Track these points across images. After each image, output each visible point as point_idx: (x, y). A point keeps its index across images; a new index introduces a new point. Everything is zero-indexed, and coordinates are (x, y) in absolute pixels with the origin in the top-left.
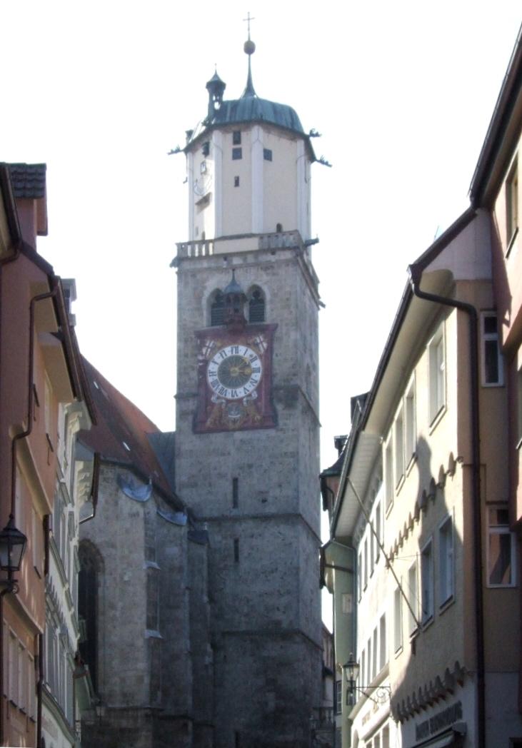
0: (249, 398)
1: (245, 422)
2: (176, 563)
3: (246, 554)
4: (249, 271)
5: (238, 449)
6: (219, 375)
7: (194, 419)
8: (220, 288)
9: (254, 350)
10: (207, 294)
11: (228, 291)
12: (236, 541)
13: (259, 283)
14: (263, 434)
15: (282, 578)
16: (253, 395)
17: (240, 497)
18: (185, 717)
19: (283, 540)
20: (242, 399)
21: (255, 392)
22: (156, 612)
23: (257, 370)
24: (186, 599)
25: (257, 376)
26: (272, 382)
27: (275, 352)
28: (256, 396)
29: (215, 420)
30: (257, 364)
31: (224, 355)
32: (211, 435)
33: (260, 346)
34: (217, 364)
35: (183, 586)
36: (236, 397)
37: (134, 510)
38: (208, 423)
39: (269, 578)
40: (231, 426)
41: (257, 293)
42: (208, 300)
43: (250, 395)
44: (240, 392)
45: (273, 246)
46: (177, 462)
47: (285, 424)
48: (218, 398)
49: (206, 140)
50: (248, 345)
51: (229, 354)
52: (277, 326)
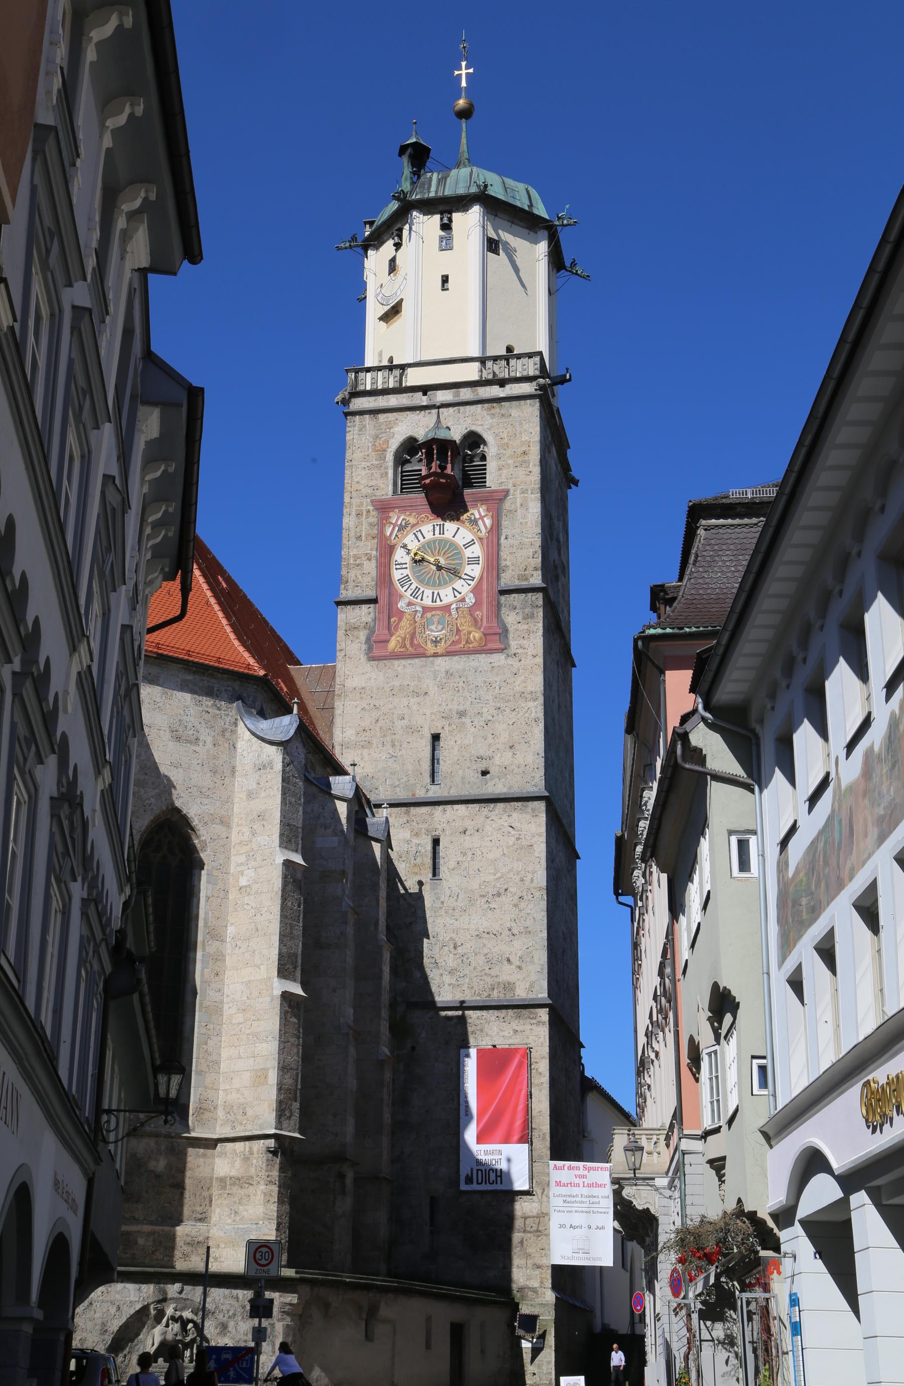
3: (452, 864)
7: (368, 640)
8: (416, 436)
9: (470, 531)
10: (394, 444)
11: (430, 436)
12: (436, 842)
14: (483, 660)
15: (516, 906)
17: (443, 767)
18: (339, 1158)
19: (518, 839)
21: (472, 595)
23: (474, 561)
25: (476, 571)
26: (498, 578)
27: (504, 532)
28: (473, 601)
29: (404, 639)
30: (476, 551)
31: (420, 537)
32: (396, 662)
33: (480, 523)
36: (438, 603)
37: (264, 758)
38: (392, 644)
39: (492, 906)
40: (431, 649)
41: (474, 440)
44: (447, 596)
45: (501, 376)
49: (399, 226)
51: (429, 536)
52: (506, 493)
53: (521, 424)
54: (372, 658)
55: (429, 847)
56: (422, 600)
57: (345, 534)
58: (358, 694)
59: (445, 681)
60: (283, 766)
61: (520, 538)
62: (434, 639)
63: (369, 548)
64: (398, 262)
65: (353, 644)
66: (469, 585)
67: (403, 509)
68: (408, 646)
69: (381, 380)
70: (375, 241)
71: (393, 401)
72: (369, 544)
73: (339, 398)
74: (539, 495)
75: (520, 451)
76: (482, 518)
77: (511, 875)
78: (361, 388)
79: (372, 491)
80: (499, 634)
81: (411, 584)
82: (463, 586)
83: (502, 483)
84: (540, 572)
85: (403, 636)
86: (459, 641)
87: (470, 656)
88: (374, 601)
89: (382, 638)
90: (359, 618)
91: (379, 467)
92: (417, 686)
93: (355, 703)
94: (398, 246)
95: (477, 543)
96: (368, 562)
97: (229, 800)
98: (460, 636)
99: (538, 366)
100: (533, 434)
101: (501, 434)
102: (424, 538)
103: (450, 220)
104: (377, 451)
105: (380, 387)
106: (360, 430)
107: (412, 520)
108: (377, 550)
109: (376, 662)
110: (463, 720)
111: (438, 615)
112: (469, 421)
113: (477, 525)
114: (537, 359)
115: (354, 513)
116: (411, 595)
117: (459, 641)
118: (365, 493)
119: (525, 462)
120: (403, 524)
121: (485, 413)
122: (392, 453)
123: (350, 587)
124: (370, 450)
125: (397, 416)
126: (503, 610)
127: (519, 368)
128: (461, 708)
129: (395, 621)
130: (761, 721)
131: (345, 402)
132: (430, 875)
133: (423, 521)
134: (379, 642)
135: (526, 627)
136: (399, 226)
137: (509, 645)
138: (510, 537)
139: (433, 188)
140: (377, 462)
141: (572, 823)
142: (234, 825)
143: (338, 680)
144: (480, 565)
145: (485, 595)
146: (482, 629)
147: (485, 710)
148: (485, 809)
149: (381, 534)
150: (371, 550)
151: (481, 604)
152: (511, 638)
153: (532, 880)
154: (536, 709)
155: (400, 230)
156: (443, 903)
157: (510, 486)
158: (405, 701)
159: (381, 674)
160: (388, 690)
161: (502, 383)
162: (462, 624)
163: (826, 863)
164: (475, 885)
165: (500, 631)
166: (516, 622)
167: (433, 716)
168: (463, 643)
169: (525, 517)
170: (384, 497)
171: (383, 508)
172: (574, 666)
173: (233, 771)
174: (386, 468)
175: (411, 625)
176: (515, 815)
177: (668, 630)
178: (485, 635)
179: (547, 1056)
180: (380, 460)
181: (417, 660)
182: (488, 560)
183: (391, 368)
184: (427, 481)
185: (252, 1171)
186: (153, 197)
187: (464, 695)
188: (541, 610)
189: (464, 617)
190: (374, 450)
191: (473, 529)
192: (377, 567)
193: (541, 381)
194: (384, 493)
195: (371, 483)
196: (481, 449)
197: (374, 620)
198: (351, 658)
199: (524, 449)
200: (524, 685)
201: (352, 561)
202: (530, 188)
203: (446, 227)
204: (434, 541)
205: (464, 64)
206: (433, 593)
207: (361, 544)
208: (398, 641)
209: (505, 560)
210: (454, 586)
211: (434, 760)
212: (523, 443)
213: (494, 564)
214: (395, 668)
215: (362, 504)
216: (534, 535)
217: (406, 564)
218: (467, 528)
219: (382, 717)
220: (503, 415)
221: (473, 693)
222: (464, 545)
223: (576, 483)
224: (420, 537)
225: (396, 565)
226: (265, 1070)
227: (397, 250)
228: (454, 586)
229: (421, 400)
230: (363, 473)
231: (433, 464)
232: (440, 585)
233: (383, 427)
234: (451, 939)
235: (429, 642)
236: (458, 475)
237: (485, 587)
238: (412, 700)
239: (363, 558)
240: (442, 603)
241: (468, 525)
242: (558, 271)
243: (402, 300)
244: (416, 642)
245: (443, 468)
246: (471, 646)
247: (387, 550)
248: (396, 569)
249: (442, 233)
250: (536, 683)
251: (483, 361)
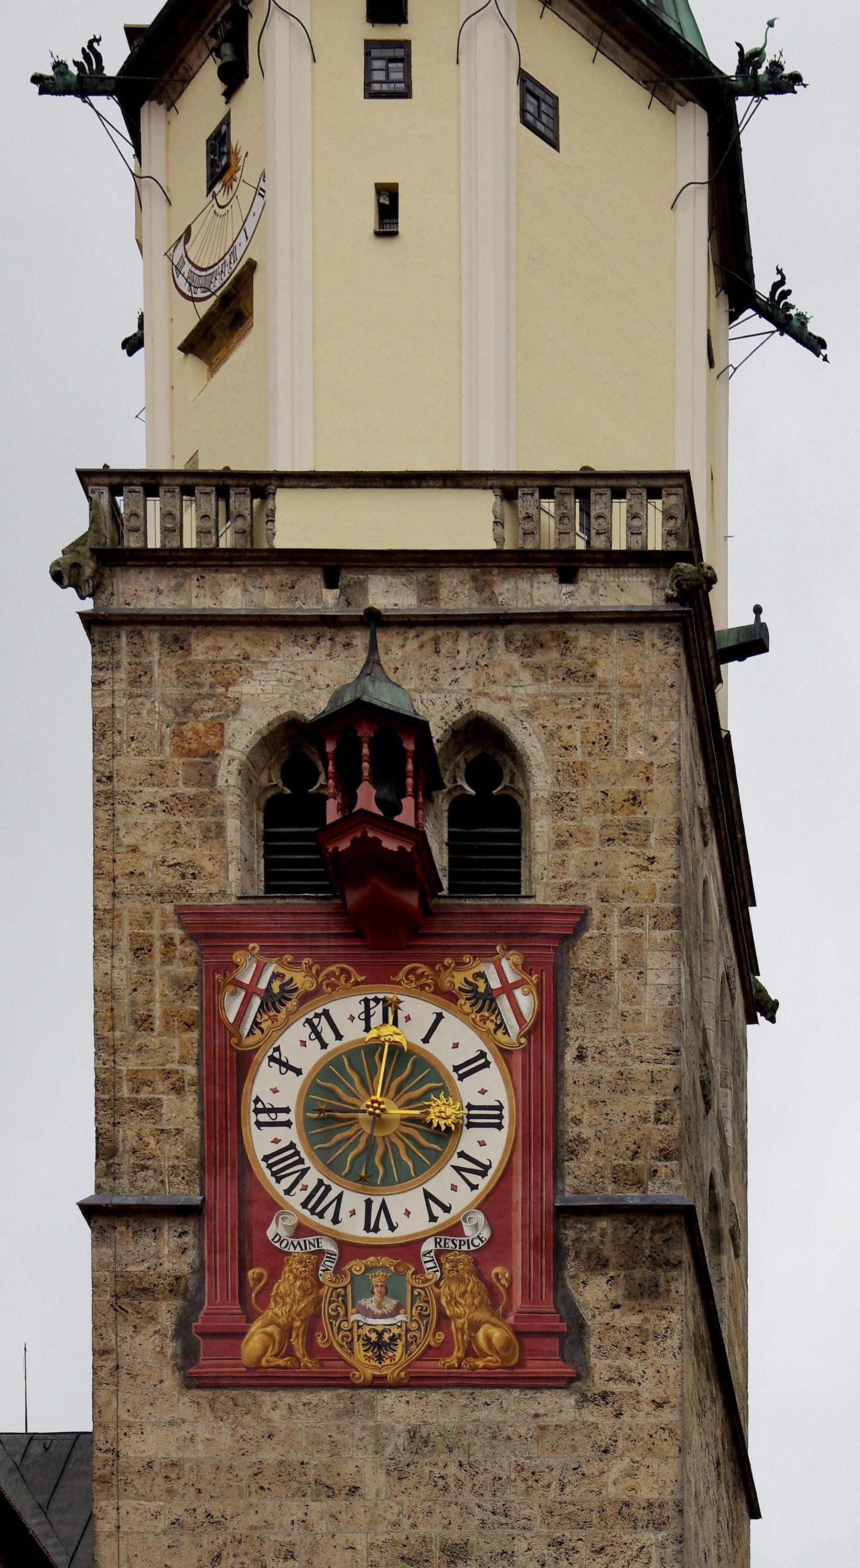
1: (429, 1352)
4: (446, 646)
6: (307, 1125)
7: (182, 1328)
9: (474, 1025)
13: (497, 712)
16: (468, 1231)
21: (480, 1217)
28: (486, 1234)
29: (287, 1331)
31: (328, 1034)
32: (267, 1398)
33: (503, 1003)
34: (298, 1072)
36: (384, 1232)
43: (455, 1230)
47: (622, 1376)
48: (301, 1230)
50: (449, 997)
51: (354, 1032)
53: (622, 705)
56: (336, 1220)
58: (160, 1480)
59: (406, 1458)
61: (619, 1060)
62: (374, 1337)
63: (176, 1055)
64: (236, 137)
65: (139, 1338)
66: (474, 1187)
68: (300, 1352)
72: (176, 1043)
75: (620, 791)
76: (508, 989)
78: (132, 542)
79: (177, 881)
80: (561, 1335)
81: (304, 1172)
82: (454, 1188)
83: (567, 887)
85: (282, 1320)
86: (445, 1349)
87: (477, 1392)
89: (223, 1323)
90: (152, 1262)
91: (196, 805)
92: (328, 1467)
93: (153, 1506)
95: (493, 1065)
96: (173, 1096)
98: (448, 1335)
100: (661, 741)
101: (564, 732)
102: (339, 1037)
104: (190, 753)
105: (190, 541)
106: (135, 681)
107: (301, 980)
108: (198, 1063)
109: (208, 1393)
111: (383, 1268)
112: (468, 681)
113: (494, 1009)
115: (125, 945)
116: (304, 1205)
118: (157, 884)
119: (634, 826)
120: (276, 989)
121: (514, 660)
122: (235, 766)
123: (124, 1168)
124: (168, 750)
125: (248, 648)
126: (571, 1266)
128: (455, 1536)
129: (260, 1277)
133: (334, 986)
134: (213, 1335)
135: (635, 1320)
137: (588, 1370)
138: (590, 1053)
140: (191, 791)
144: (505, 1131)
145: (518, 1217)
146: (511, 1319)
147: (520, 1546)
150: (183, 1061)
151: (508, 1244)
152: (593, 1350)
157: (591, 900)
158: (294, 1509)
159: (225, 1429)
160: (245, 1474)
162: (453, 1301)
165: (563, 1326)
166: (605, 1305)
167: (376, 1554)
168: (458, 1353)
169: (633, 997)
170: (214, 902)
174: (219, 811)
175: (305, 1292)
178: (520, 1334)
180: (199, 784)
181: (325, 1395)
182: (526, 1118)
187: (461, 1500)
189: (461, 1280)
191: (484, 1020)
192: (200, 1114)
194: (214, 889)
195: (180, 855)
196: (506, 782)
197: (199, 1270)
198: (134, 1377)
199: (634, 784)
200: (630, 1482)
201: (125, 1091)
206: (369, 1203)
207: (153, 1040)
208: (270, 1335)
209: (577, 1121)
210: (430, 1186)
212: (630, 768)
214: (264, 1414)
215: (149, 917)
216: (661, 1055)
217: (287, 1110)
218: (463, 1016)
219: (230, 1549)
220: (570, 673)
221: (488, 1495)
222: (456, 1069)
224: (328, 1034)
225: (257, 1111)
227: (229, 95)
228: (428, 1186)
229: (319, 599)
230: (149, 820)
232: (388, 1181)
233: (206, 678)
235: (358, 1346)
237: (518, 1195)
238: (316, 1507)
239: (161, 1086)
240: (397, 1233)
241: (467, 1008)
243: (251, 266)
244: (321, 1343)
246: (480, 1363)
248: (259, 1124)
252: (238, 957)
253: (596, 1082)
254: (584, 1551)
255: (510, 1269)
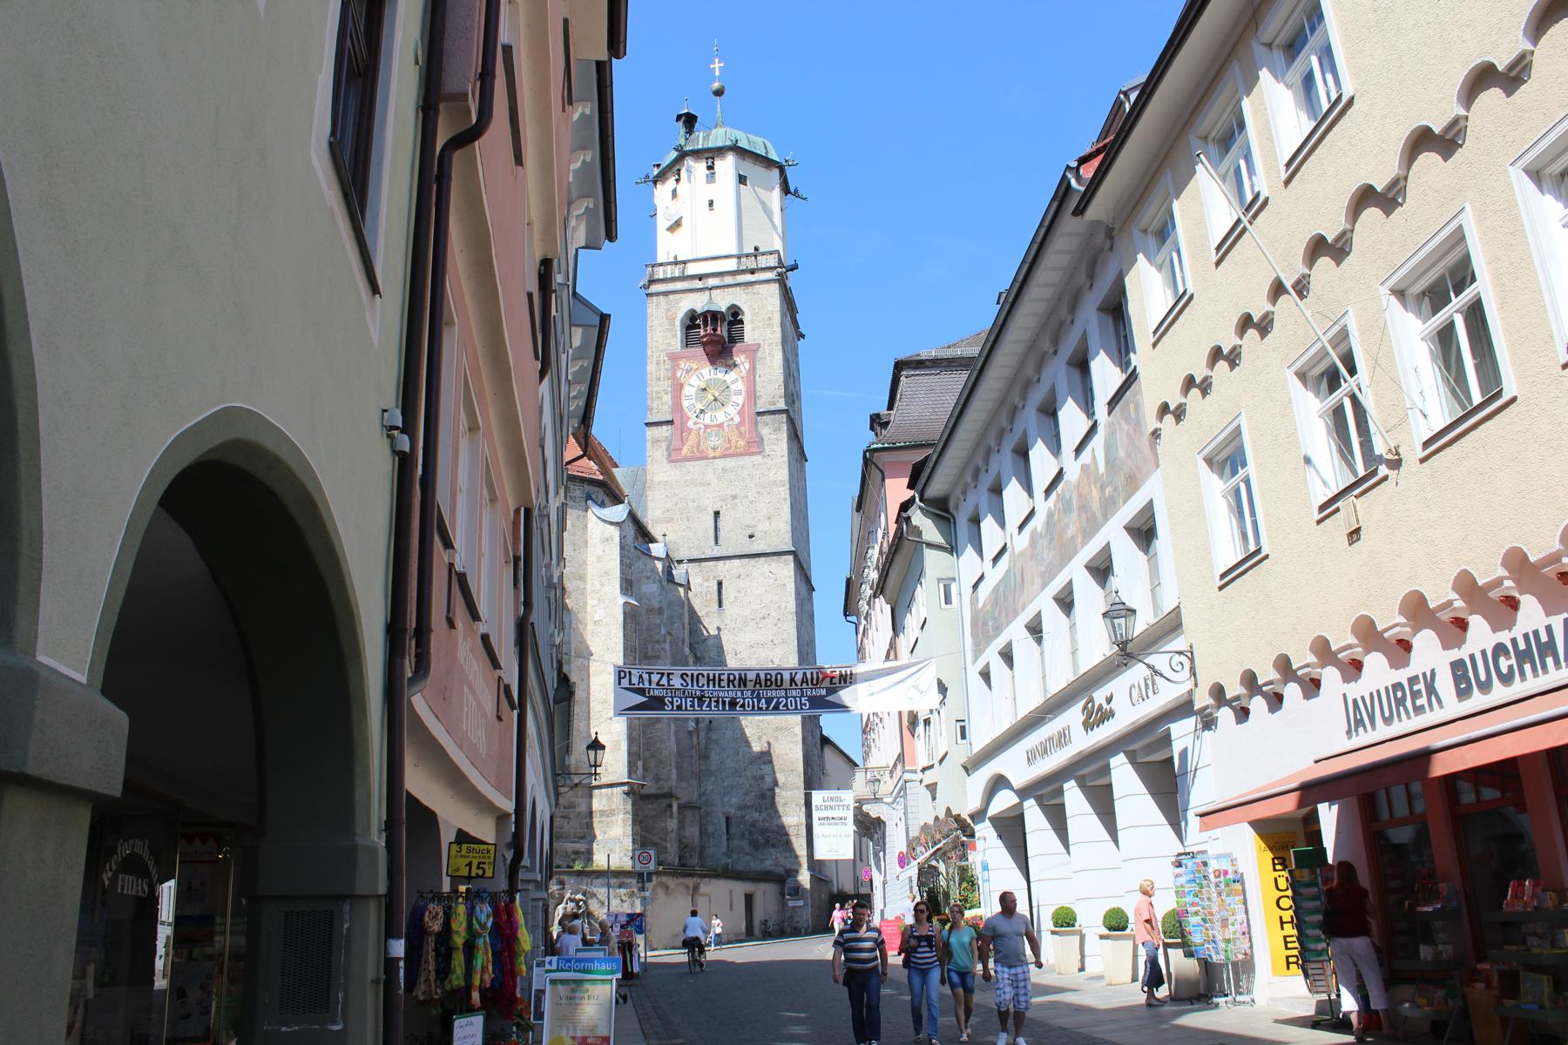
0: (730, 423)
1: (727, 449)
2: (655, 604)
3: (732, 599)
5: (720, 479)
8: (695, 308)
10: (681, 314)
12: (720, 584)
14: (747, 460)
15: (775, 625)
17: (722, 534)
18: (669, 795)
19: (776, 580)
20: (723, 424)
21: (737, 416)
22: (635, 659)
23: (738, 393)
24: (667, 646)
25: (740, 399)
26: (755, 404)
27: (758, 373)
28: (739, 420)
29: (692, 447)
30: (740, 386)
31: (701, 377)
33: (741, 366)
35: (663, 631)
36: (715, 422)
37: (607, 534)
38: (685, 451)
39: (760, 626)
40: (711, 453)
42: (682, 322)
43: (732, 419)
44: (720, 416)
46: (649, 493)
49: (678, 167)
54: (671, 461)
55: (716, 588)
57: (649, 377)
60: (620, 539)
64: (678, 191)
67: (688, 358)
69: (670, 271)
70: (660, 178)
71: (679, 286)
73: (641, 284)
74: (781, 347)
76: (742, 363)
77: (771, 605)
78: (656, 277)
84: (783, 399)
86: (730, 448)
88: (671, 422)
89: (678, 447)
94: (678, 181)
97: (584, 562)
99: (777, 260)
103: (713, 163)
105: (669, 276)
106: (657, 305)
110: (735, 501)
114: (777, 256)
115: (655, 362)
117: (730, 448)
119: (770, 324)
121: (742, 292)
126: (760, 426)
127: (764, 261)
128: (734, 493)
130: (957, 508)
131: (646, 287)
132: (717, 607)
136: (678, 167)
139: (701, 143)
141: (810, 568)
142: (589, 580)
143: (648, 477)
148: (752, 561)
149: (674, 378)
151: (744, 422)
153: (786, 608)
154: (784, 492)
155: (679, 170)
156: (726, 625)
157: (761, 341)
161: (752, 272)
163: (1006, 600)
164: (747, 612)
171: (674, 358)
172: (806, 461)
173: (586, 542)
174: (676, 330)
176: (773, 564)
177: (886, 445)
178: (748, 443)
179: (800, 723)
181: (702, 461)
183: (676, 263)
184: (705, 340)
185: (614, 807)
186: (591, 206)
188: (785, 425)
190: (667, 319)
193: (779, 270)
197: (672, 435)
201: (654, 395)
202: (765, 141)
203: (710, 168)
204: (711, 380)
205: (717, 60)
210: (726, 410)
211: (716, 528)
212: (769, 312)
213: (752, 395)
223: (803, 336)
224: (701, 377)
226: (619, 741)
231: (708, 328)
232: (716, 409)
234: (733, 649)
235: (710, 449)
236: (725, 334)
237: (746, 410)
242: (786, 195)
245: (715, 330)
247: (678, 387)
249: (707, 172)
250: (784, 474)
251: (739, 257)
252: (680, 362)
253: (764, 382)
254: (765, 493)
255: (745, 426)
